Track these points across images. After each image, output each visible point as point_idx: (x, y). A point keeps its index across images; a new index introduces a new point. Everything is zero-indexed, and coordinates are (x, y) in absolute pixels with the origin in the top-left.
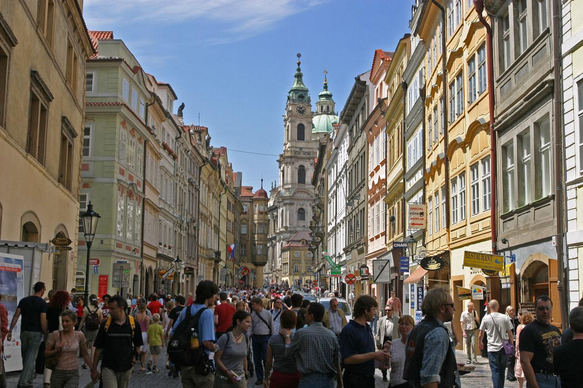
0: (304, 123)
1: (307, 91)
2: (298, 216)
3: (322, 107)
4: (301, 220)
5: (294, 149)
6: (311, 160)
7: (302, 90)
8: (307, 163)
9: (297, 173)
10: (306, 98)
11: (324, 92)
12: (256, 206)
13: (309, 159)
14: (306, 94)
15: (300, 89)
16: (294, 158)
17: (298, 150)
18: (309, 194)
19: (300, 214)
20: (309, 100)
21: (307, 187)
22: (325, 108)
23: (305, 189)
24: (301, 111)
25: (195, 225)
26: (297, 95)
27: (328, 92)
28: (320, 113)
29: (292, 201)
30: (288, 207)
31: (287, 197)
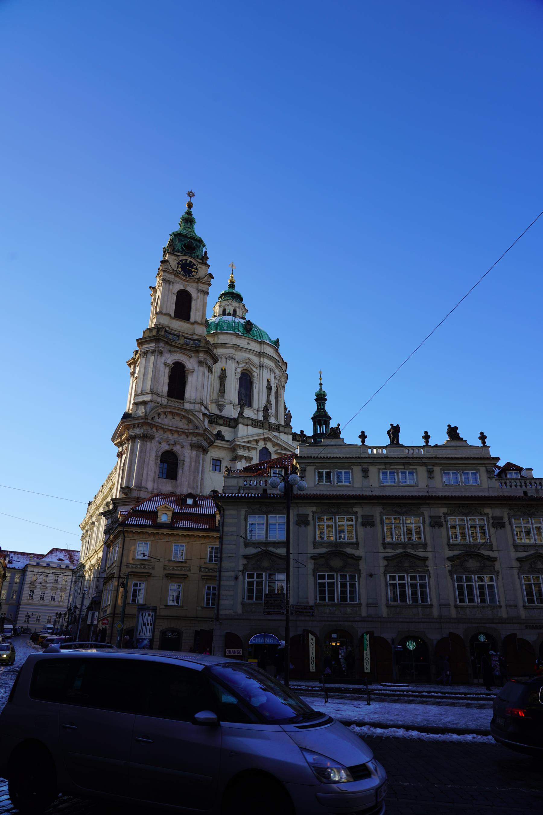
0: (192, 289)
4: (167, 478)
6: (201, 355)
8: (191, 360)
9: (167, 375)
11: (231, 290)
14: (199, 247)
15: (189, 236)
18: (190, 421)
19: (165, 465)
21: (187, 406)
23: (182, 409)
24: (187, 270)
29: (150, 431)
31: (138, 418)
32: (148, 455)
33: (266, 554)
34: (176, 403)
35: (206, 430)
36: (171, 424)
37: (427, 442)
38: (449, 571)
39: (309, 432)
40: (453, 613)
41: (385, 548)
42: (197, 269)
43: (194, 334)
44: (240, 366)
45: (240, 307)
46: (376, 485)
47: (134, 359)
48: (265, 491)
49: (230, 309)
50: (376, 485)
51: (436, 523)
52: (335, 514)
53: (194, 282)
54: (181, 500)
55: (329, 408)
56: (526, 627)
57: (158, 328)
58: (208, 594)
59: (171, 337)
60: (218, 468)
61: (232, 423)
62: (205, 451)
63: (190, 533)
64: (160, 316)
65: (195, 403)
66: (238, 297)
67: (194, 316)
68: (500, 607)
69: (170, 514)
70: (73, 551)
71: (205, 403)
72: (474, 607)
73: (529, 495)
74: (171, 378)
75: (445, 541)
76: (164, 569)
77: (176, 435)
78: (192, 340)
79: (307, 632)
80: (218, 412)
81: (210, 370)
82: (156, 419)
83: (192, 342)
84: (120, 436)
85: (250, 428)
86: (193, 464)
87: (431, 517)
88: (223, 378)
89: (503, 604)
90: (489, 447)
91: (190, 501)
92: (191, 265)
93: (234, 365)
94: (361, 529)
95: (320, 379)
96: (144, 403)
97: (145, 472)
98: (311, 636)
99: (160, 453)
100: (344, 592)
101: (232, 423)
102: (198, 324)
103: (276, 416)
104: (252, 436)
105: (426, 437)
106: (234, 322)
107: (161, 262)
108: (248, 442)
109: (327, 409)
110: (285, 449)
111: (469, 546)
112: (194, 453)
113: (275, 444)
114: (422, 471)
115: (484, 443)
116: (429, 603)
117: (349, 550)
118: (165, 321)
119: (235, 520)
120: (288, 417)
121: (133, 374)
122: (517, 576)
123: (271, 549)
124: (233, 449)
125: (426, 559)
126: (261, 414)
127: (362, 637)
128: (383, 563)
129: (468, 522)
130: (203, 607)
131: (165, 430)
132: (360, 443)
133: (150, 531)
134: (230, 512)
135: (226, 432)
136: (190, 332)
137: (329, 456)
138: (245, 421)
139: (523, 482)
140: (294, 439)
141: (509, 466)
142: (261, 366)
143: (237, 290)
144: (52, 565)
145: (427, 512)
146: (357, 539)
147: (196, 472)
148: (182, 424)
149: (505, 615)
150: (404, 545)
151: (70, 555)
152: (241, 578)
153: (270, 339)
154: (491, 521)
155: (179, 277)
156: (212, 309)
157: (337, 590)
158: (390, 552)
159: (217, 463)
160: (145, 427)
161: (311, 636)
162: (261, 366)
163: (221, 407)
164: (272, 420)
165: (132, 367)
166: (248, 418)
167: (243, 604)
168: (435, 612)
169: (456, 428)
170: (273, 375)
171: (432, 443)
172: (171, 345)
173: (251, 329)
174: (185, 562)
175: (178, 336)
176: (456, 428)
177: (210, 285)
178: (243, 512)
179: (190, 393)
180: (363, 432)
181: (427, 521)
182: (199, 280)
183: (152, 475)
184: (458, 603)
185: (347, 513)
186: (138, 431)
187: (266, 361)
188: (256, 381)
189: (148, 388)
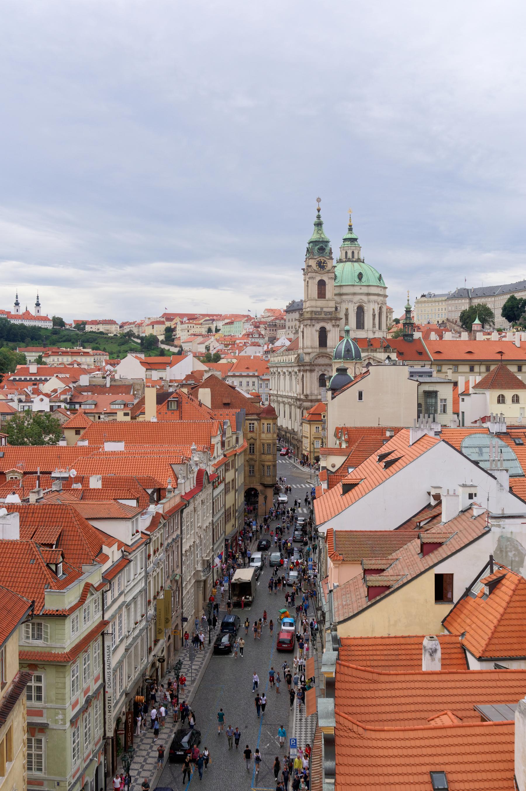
0: (325, 278)
1: (328, 242)
3: (346, 253)
5: (314, 309)
6: (333, 321)
8: (329, 324)
9: (318, 336)
10: (327, 251)
11: (349, 236)
12: (263, 424)
13: (331, 319)
14: (326, 246)
15: (321, 240)
16: (315, 320)
17: (319, 309)
20: (331, 253)
22: (350, 255)
23: (326, 353)
24: (321, 265)
25: (220, 324)
26: (317, 247)
27: (353, 236)
28: (344, 260)
30: (308, 374)
65: (332, 348)
74: (320, 337)
77: (325, 367)
96: (309, 354)
113: (374, 360)
118: (313, 303)
131: (320, 365)
162: (369, 302)
179: (330, 342)
182: (328, 272)
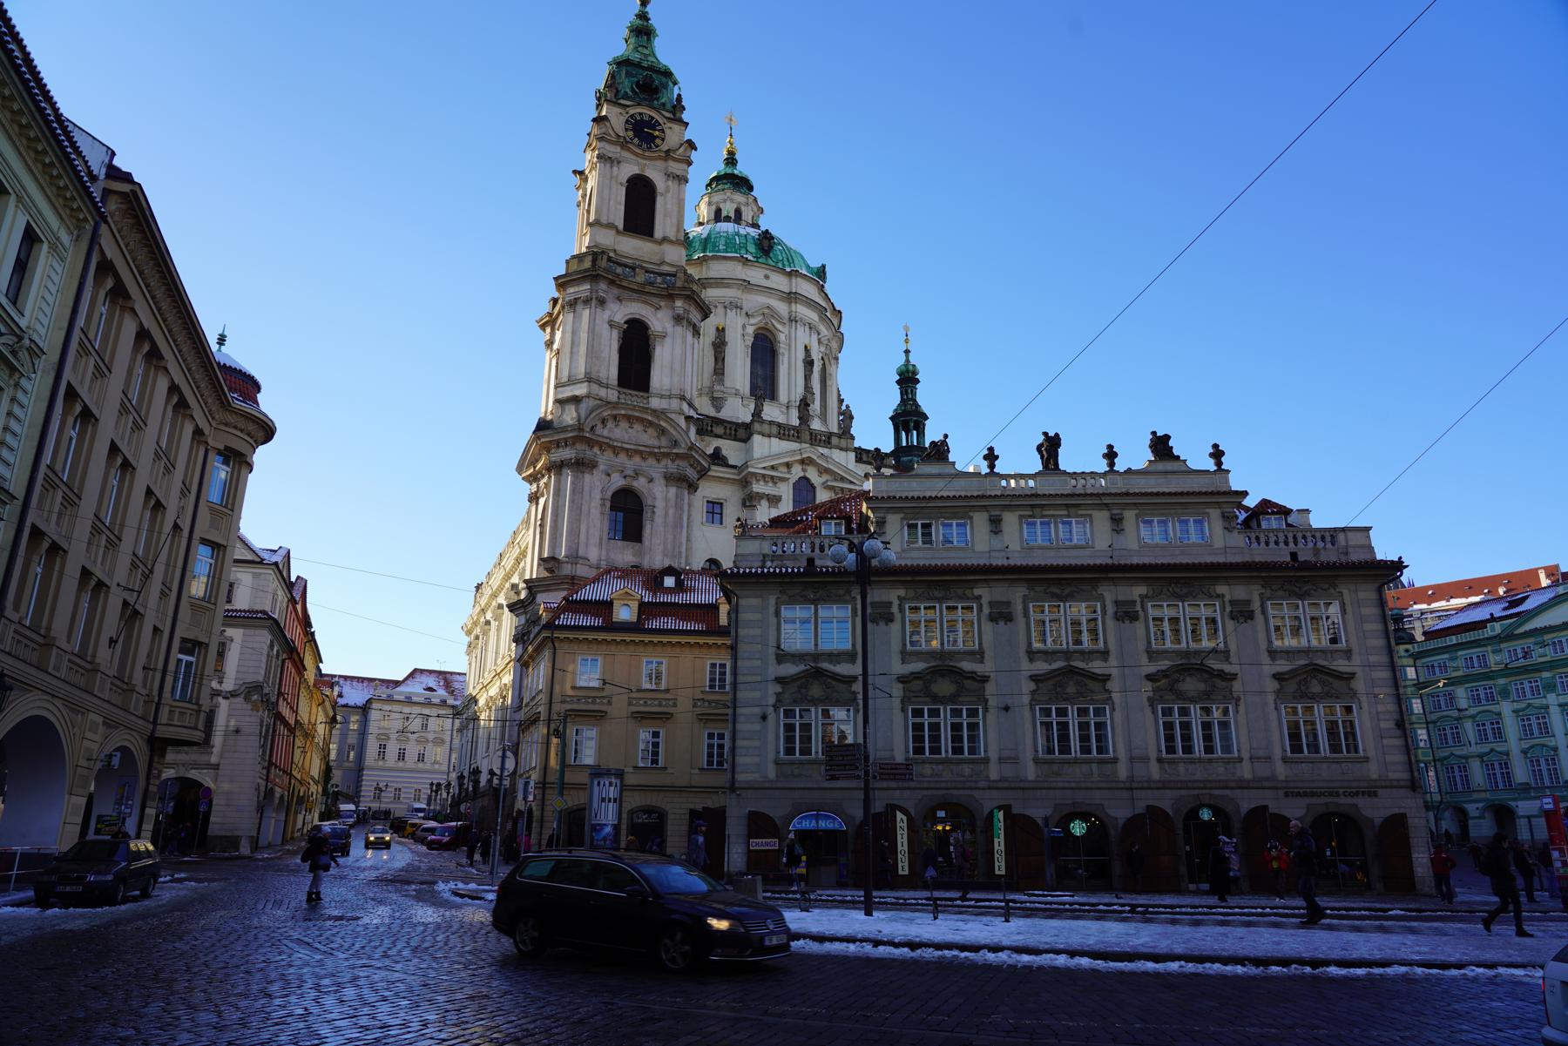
0: (655, 173)
2: (613, 522)
3: (718, 211)
4: (624, 539)
6: (679, 303)
7: (651, 68)
8: (660, 314)
9: (615, 346)
11: (729, 171)
14: (665, 86)
15: (645, 64)
18: (663, 432)
19: (620, 515)
21: (655, 403)
23: (646, 410)
24: (644, 134)
31: (564, 429)
32: (586, 497)
33: (818, 673)
34: (633, 398)
35: (692, 447)
36: (626, 438)
37: (1111, 465)
38: (1149, 699)
39: (887, 446)
40: (1155, 772)
41: (1031, 660)
42: (663, 131)
43: (663, 263)
44: (753, 321)
45: (747, 204)
46: (1015, 546)
47: (550, 314)
48: (811, 561)
49: (728, 209)
50: (1015, 546)
51: (1127, 613)
52: (940, 600)
53: (660, 158)
54: (654, 580)
55: (923, 397)
56: (1287, 795)
57: (595, 253)
58: (710, 746)
59: (619, 270)
60: (717, 517)
61: (741, 433)
62: (693, 487)
63: (674, 639)
64: (596, 228)
65: (670, 397)
66: (743, 184)
67: (662, 227)
68: (1240, 760)
69: (635, 605)
70: (451, 673)
71: (688, 396)
72: (1193, 761)
73: (1301, 559)
74: (623, 351)
75: (1142, 646)
76: (630, 704)
77: (637, 459)
78: (660, 274)
79: (892, 809)
80: (712, 412)
81: (696, 332)
82: (599, 430)
83: (659, 279)
84: (534, 463)
85: (775, 441)
86: (671, 511)
87: (1117, 603)
88: (719, 346)
89: (1246, 755)
90: (1228, 471)
91: (669, 582)
92: (652, 124)
93: (740, 320)
94: (988, 627)
95: (907, 341)
96: (575, 400)
97: (583, 528)
98: (899, 815)
99: (609, 494)
100: (957, 739)
101: (741, 433)
102: (671, 242)
103: (824, 416)
104: (779, 455)
105: (1111, 455)
106: (738, 234)
107: (594, 120)
108: (773, 468)
109: (920, 399)
110: (843, 479)
111: (1187, 654)
112: (673, 490)
113: (823, 471)
114: (1101, 518)
115: (1219, 464)
116: (1111, 754)
117: (967, 666)
118: (607, 239)
119: (758, 616)
120: (847, 417)
121: (549, 344)
122: (1272, 706)
123: (825, 665)
124: (745, 483)
125: (1106, 678)
126: (794, 413)
127: (991, 815)
128: (1027, 687)
129: (1185, 610)
130: (702, 769)
131: (616, 451)
132: (985, 470)
133: (600, 636)
134: (750, 603)
135: (730, 449)
136: (656, 259)
137: (928, 494)
138: (766, 429)
139: (1290, 536)
140: (859, 460)
141: (1266, 506)
142: (793, 320)
143: (741, 169)
144: (415, 699)
145: (1110, 593)
146: (980, 644)
147: (677, 525)
148: (647, 438)
149: (1248, 775)
150: (1067, 654)
151: (446, 680)
152: (771, 718)
153: (808, 267)
154: (1228, 609)
155: (629, 150)
156: (692, 208)
157: (946, 735)
158: (1042, 667)
159: (715, 510)
160: (578, 446)
161: (899, 815)
162: (793, 320)
163: (717, 402)
164: (816, 425)
165: (548, 330)
166: (771, 423)
167: (777, 763)
168: (1122, 771)
169: (1167, 437)
170: (815, 337)
171: (1120, 465)
172: (620, 286)
173: (771, 247)
174: (667, 691)
175: (633, 269)
176: (1167, 437)
177: (690, 163)
178: (772, 601)
179: (660, 377)
180: (991, 449)
181: (1110, 609)
182: (668, 155)
183: (597, 534)
184: (1164, 754)
185: (963, 598)
186: (567, 454)
187: (802, 311)
188: (782, 349)
189: (581, 371)
